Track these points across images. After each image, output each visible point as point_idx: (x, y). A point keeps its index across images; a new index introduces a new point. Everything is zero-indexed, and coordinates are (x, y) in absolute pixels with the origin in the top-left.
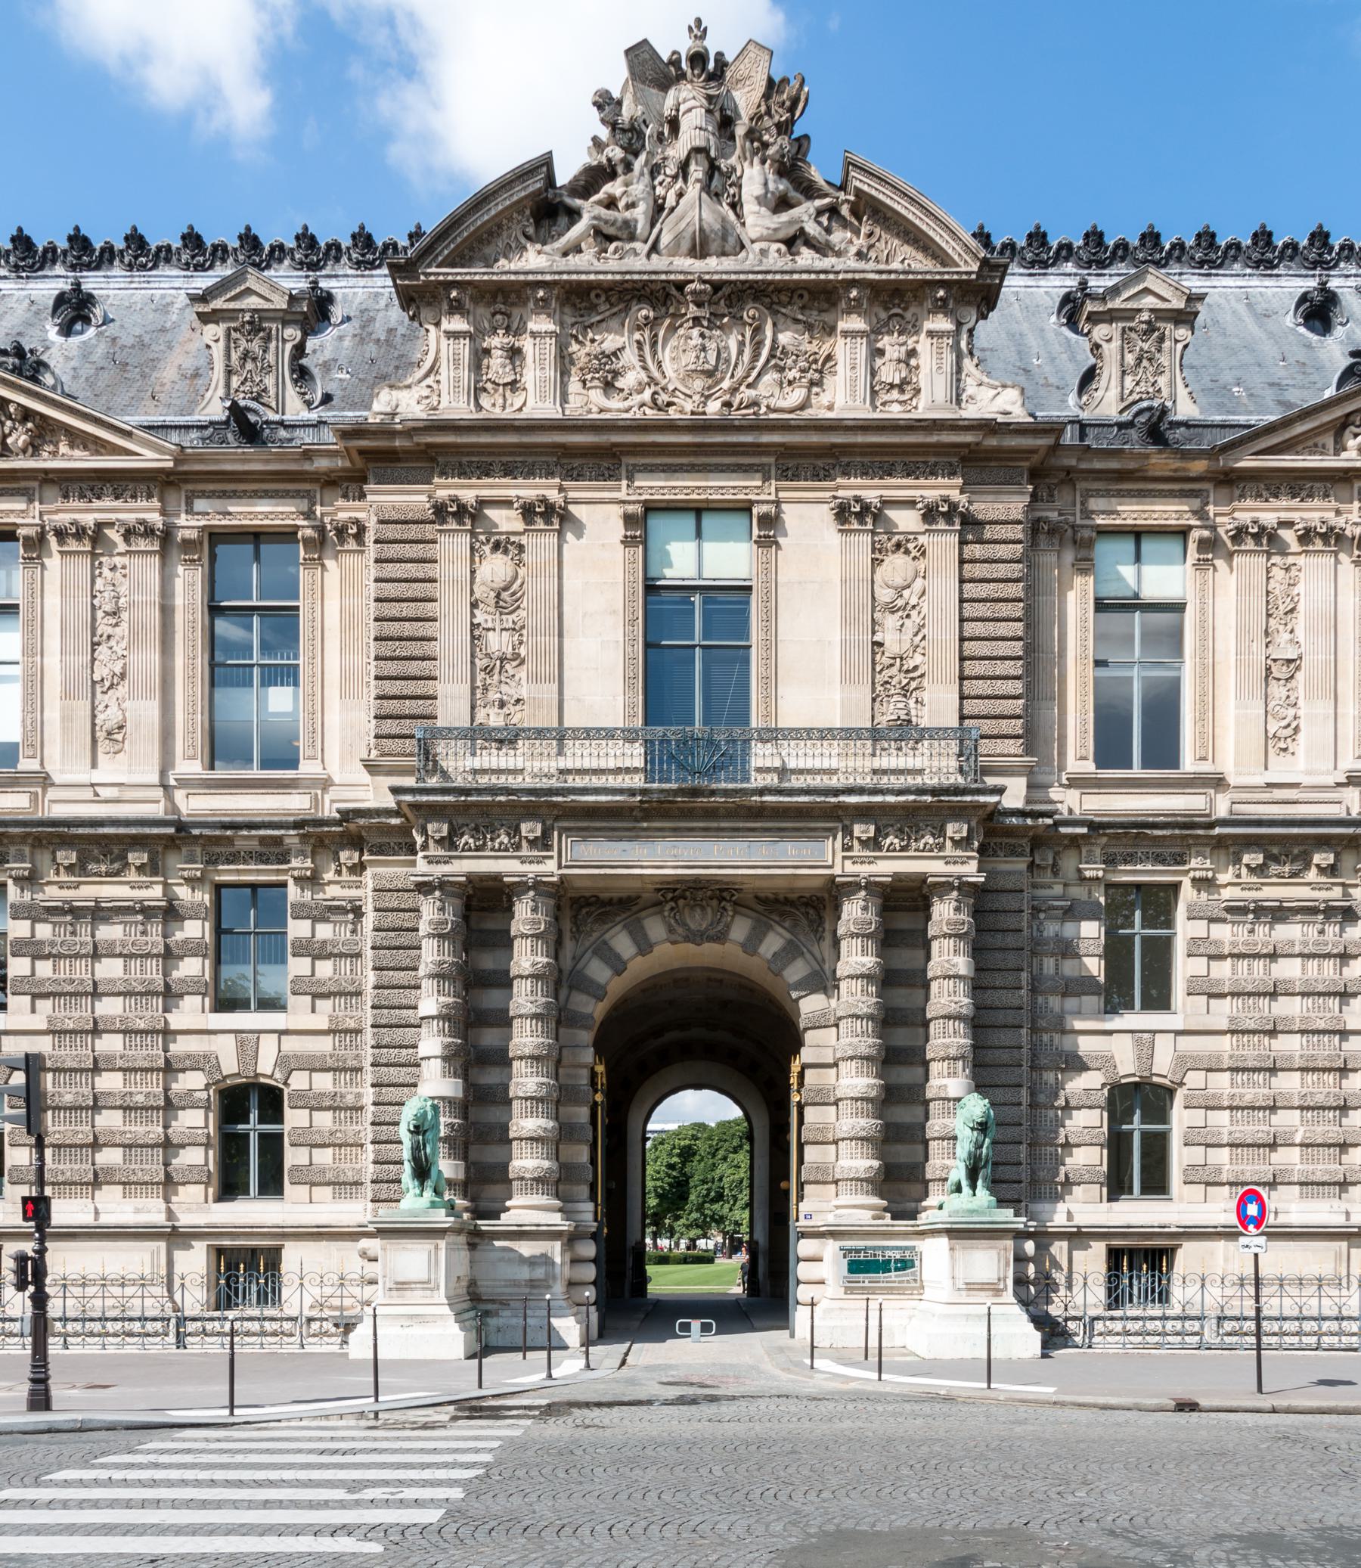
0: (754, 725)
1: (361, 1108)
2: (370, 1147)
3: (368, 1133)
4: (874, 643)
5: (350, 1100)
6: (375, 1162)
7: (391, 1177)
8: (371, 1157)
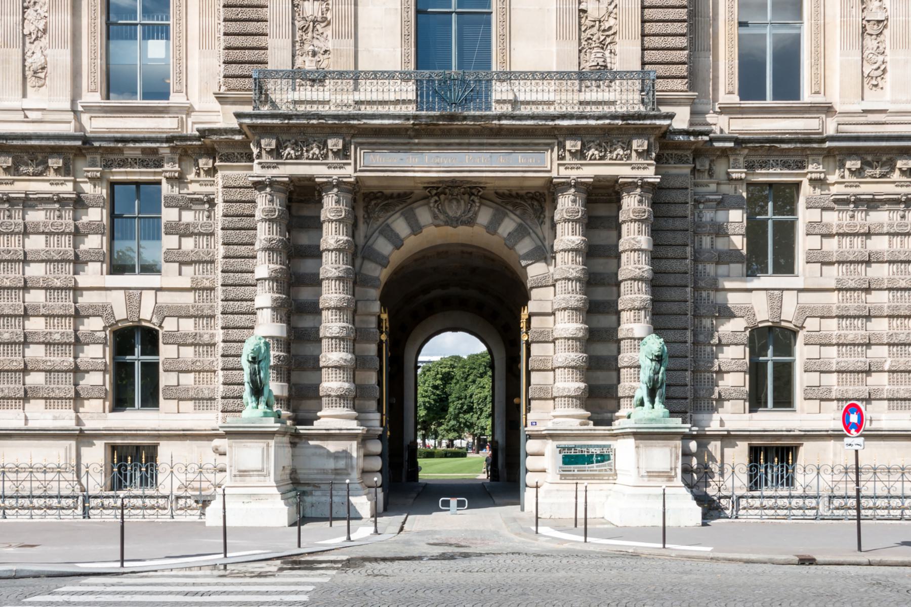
0: (494, 69)
1: (214, 344)
2: (221, 373)
3: (219, 363)
4: (580, 11)
5: (206, 339)
6: (224, 384)
7: (236, 394)
8: (221, 380)
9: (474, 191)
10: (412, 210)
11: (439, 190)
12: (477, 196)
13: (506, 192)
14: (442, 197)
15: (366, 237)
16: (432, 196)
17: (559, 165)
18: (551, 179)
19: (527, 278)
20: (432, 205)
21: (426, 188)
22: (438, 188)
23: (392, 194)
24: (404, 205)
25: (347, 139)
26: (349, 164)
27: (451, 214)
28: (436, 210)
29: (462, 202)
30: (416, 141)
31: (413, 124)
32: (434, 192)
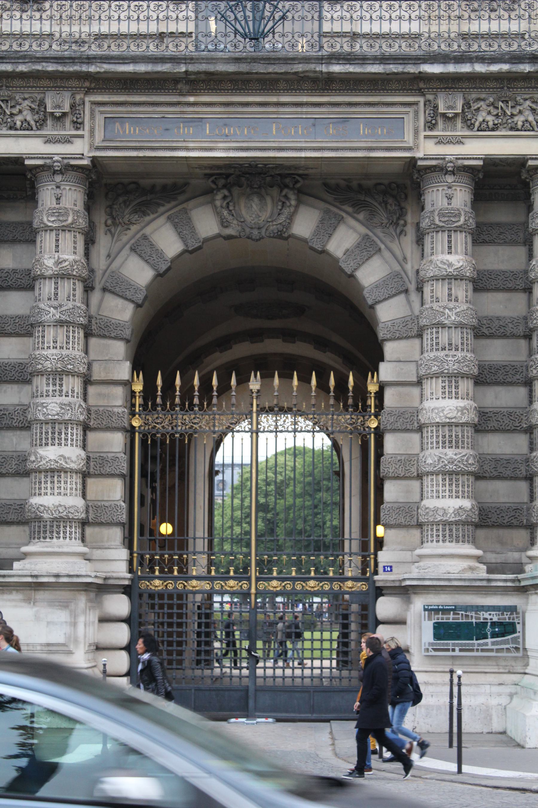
9: (287, 180)
11: (231, 179)
14: (236, 191)
16: (218, 189)
19: (377, 324)
20: (218, 203)
21: (208, 176)
22: (228, 176)
24: (173, 203)
25: (78, 97)
27: (248, 219)
28: (225, 213)
29: (269, 200)
30: (192, 99)
31: (186, 72)
32: (222, 182)
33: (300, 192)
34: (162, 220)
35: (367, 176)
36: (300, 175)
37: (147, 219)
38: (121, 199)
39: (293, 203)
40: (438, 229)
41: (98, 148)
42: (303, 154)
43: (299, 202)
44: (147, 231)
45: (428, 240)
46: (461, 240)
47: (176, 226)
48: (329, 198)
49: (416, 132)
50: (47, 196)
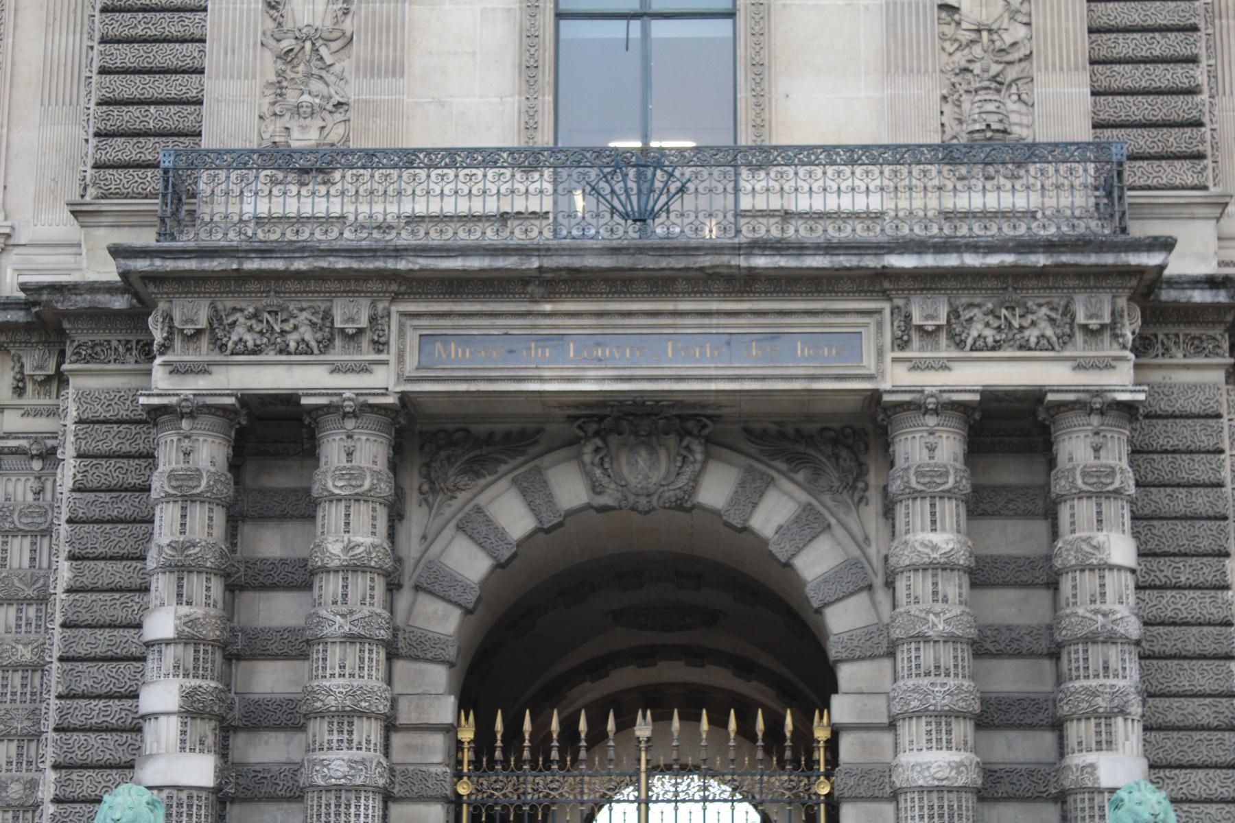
10: (538, 471)
11: (606, 423)
12: (698, 437)
13: (773, 428)
15: (424, 537)
16: (588, 438)
17: (895, 360)
18: (876, 395)
20: (587, 458)
21: (572, 418)
22: (601, 418)
23: (491, 435)
24: (520, 459)
26: (386, 363)
33: (709, 441)
34: (504, 483)
35: (809, 418)
36: (709, 417)
37: (482, 482)
38: (443, 454)
39: (699, 457)
40: (916, 495)
41: (410, 380)
42: (713, 386)
43: (708, 456)
44: (482, 500)
45: (900, 511)
46: (950, 510)
47: (524, 493)
48: (753, 449)
49: (880, 353)
50: (333, 450)
